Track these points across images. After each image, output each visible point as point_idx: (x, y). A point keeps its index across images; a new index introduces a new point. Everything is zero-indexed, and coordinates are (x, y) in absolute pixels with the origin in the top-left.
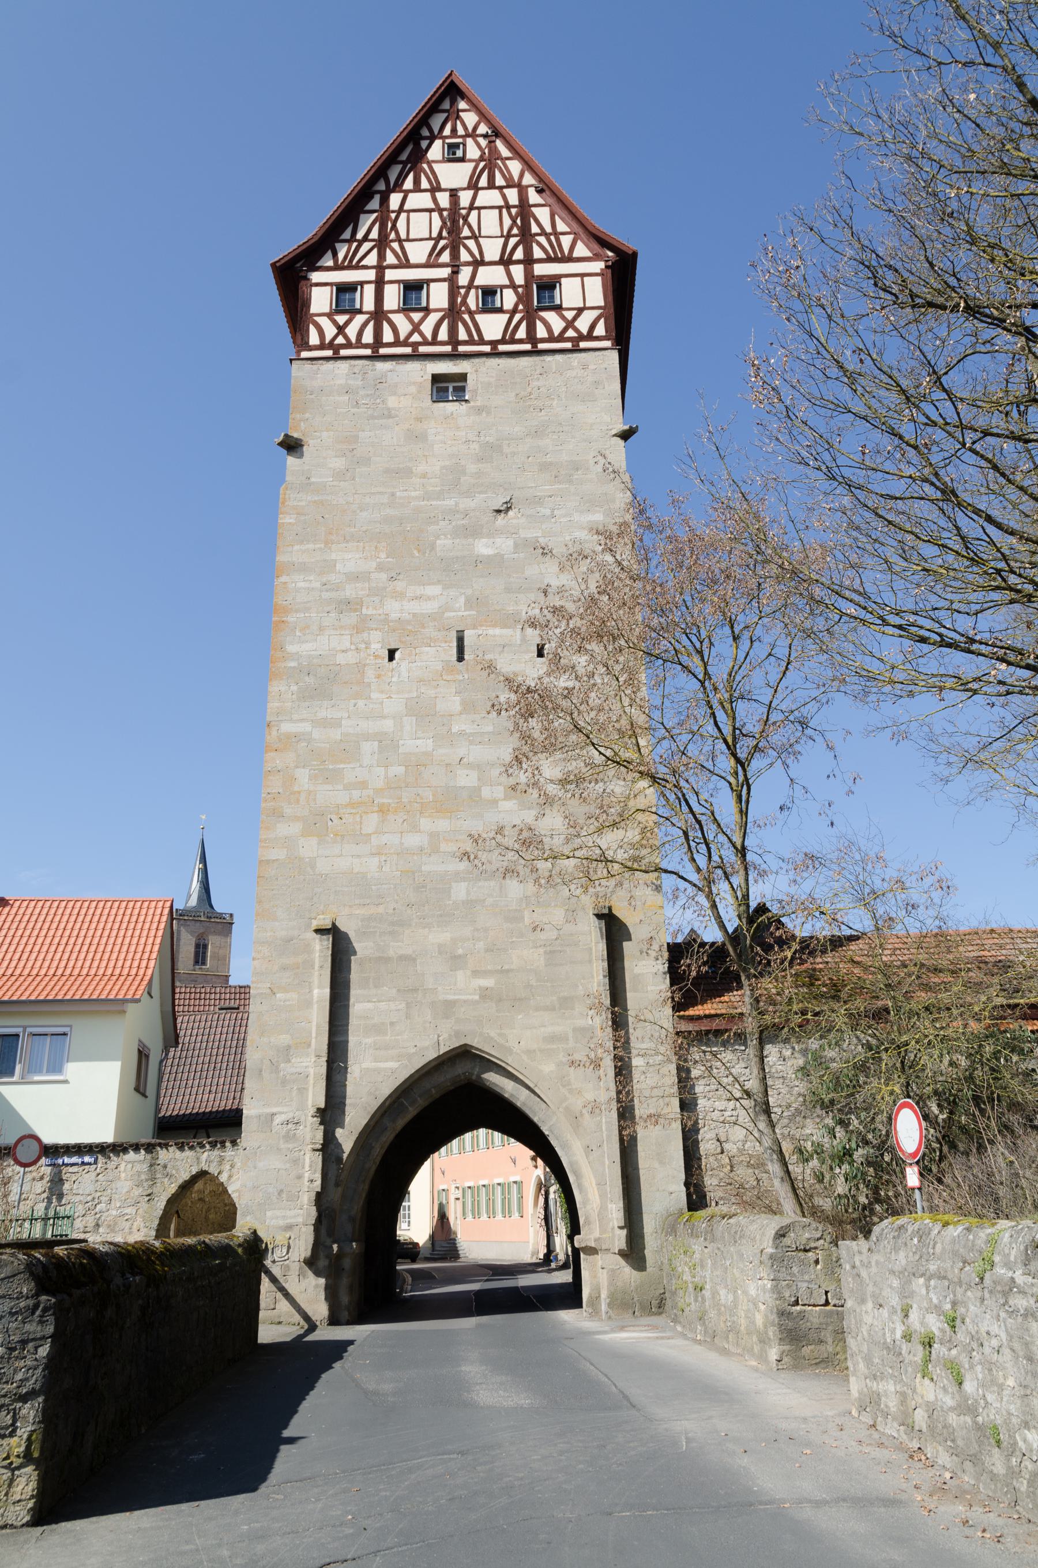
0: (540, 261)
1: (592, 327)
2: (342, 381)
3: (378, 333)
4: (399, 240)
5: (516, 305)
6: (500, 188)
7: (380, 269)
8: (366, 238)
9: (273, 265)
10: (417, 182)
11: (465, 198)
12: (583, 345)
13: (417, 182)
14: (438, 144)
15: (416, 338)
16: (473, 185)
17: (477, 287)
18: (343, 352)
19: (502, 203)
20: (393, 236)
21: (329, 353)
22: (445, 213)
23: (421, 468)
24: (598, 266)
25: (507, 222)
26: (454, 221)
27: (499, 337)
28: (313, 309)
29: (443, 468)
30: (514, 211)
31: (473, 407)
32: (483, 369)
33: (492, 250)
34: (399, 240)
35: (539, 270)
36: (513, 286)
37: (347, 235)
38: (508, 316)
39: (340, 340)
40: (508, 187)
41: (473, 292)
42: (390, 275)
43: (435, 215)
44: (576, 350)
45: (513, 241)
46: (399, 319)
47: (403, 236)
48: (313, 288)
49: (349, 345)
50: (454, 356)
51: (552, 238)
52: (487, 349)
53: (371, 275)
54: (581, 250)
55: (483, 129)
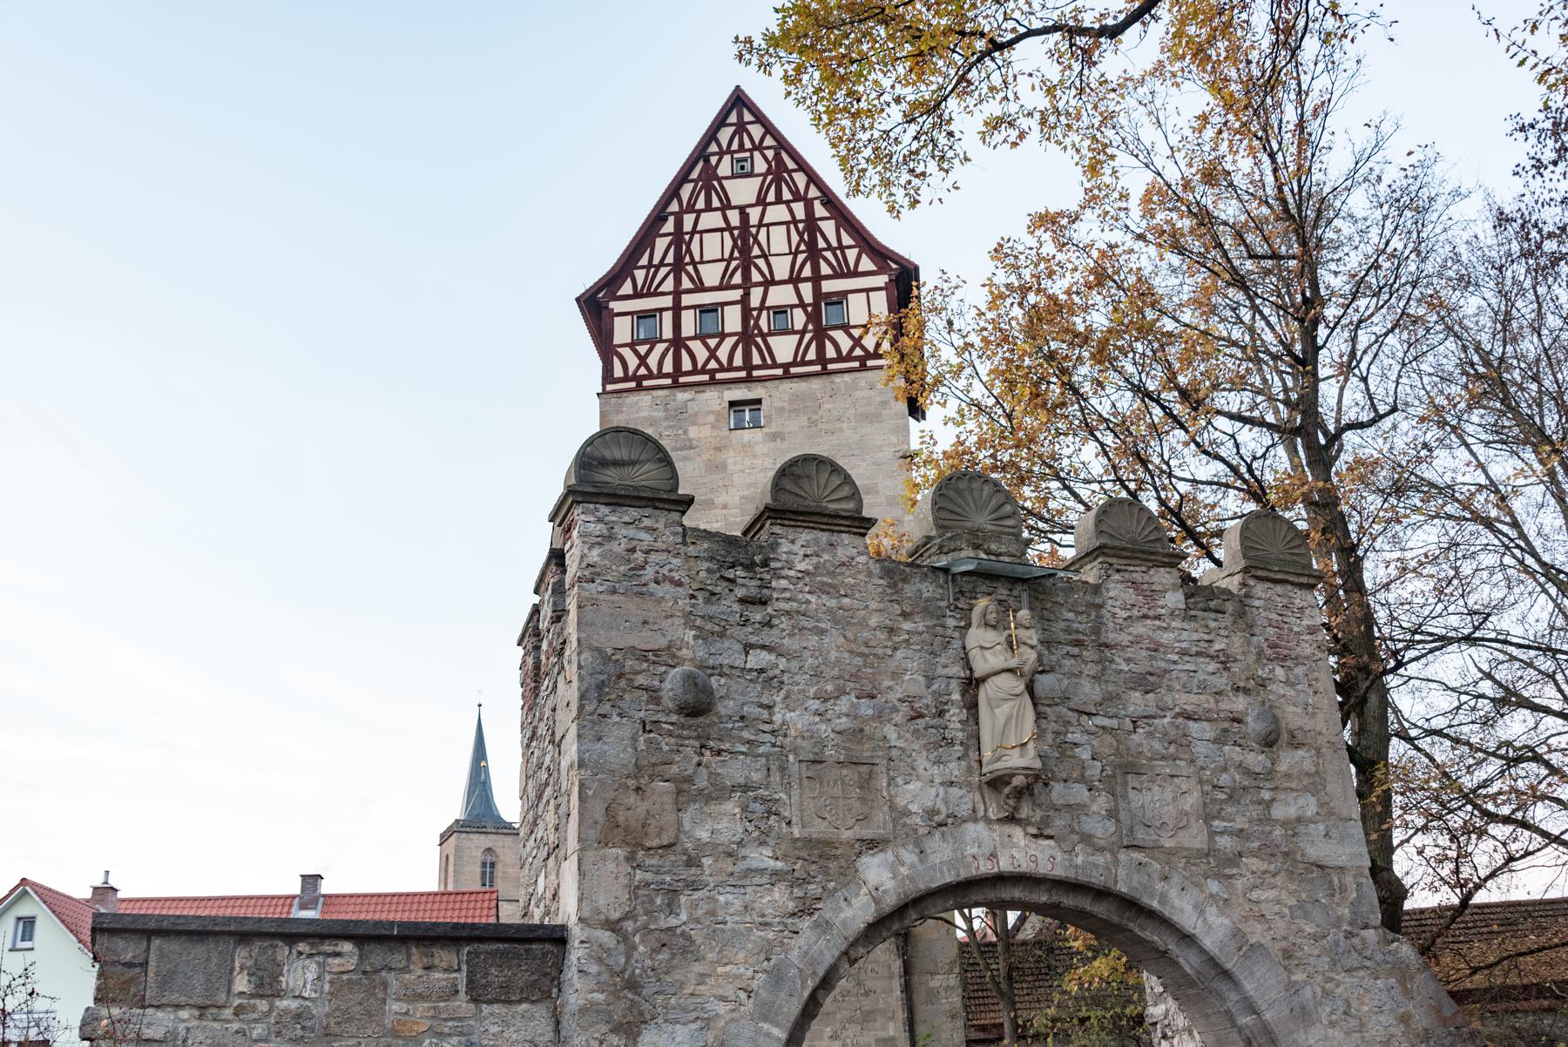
0: (828, 277)
1: (878, 345)
2: (645, 414)
4: (693, 263)
5: (806, 326)
6: (788, 203)
7: (677, 294)
8: (662, 264)
9: (578, 300)
10: (708, 201)
11: (754, 215)
12: (870, 363)
13: (708, 201)
14: (727, 158)
15: (713, 365)
16: (761, 201)
17: (769, 308)
18: (645, 383)
20: (687, 259)
22: (736, 232)
23: (722, 499)
24: (881, 280)
25: (795, 238)
26: (745, 241)
27: (790, 359)
28: (616, 342)
29: (743, 497)
30: (801, 226)
31: (767, 434)
32: (775, 393)
33: (782, 268)
34: (693, 263)
35: (828, 286)
36: (802, 305)
37: (644, 261)
38: (797, 337)
39: (643, 371)
41: (765, 313)
42: (687, 300)
43: (726, 234)
44: (863, 367)
45: (801, 257)
46: (696, 346)
47: (697, 259)
48: (616, 319)
49: (650, 376)
50: (749, 380)
52: (779, 372)
53: (667, 301)
54: (866, 264)
55: (769, 141)
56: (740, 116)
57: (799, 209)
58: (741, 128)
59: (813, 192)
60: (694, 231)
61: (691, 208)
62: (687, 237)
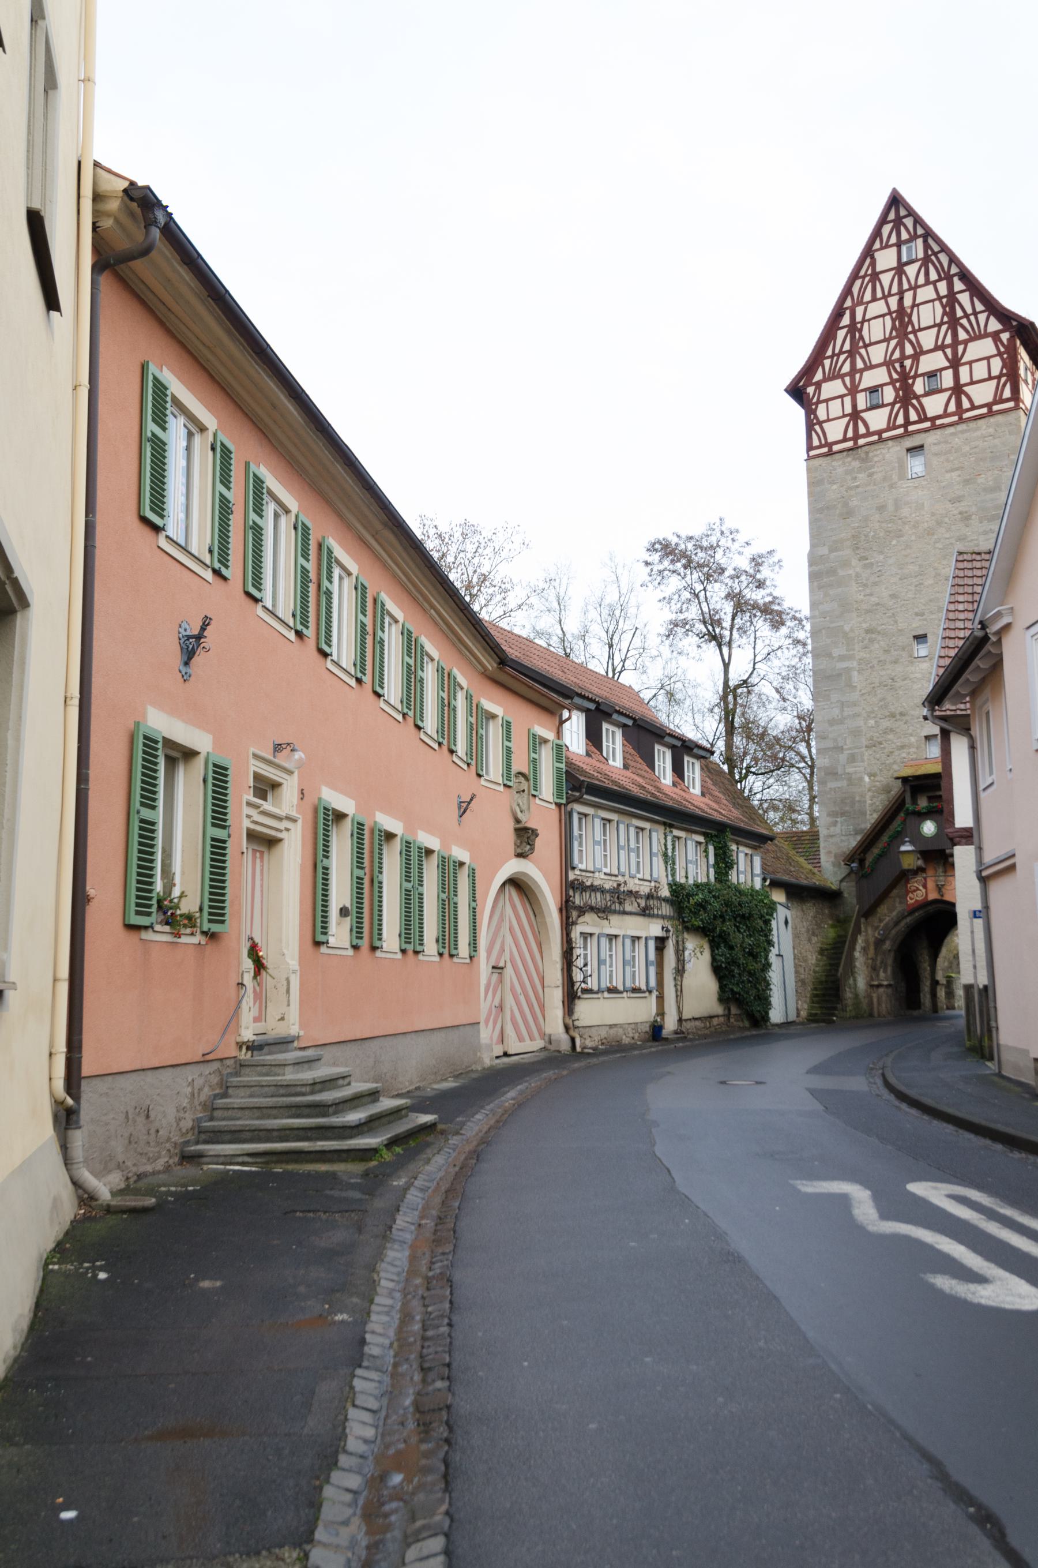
6: (934, 283)
8: (841, 352)
9: (786, 390)
21: (825, 450)
26: (902, 322)
37: (829, 353)
40: (940, 279)
51: (972, 318)
57: (943, 287)
58: (898, 222)
60: (864, 321)
61: (860, 302)
62: (859, 326)
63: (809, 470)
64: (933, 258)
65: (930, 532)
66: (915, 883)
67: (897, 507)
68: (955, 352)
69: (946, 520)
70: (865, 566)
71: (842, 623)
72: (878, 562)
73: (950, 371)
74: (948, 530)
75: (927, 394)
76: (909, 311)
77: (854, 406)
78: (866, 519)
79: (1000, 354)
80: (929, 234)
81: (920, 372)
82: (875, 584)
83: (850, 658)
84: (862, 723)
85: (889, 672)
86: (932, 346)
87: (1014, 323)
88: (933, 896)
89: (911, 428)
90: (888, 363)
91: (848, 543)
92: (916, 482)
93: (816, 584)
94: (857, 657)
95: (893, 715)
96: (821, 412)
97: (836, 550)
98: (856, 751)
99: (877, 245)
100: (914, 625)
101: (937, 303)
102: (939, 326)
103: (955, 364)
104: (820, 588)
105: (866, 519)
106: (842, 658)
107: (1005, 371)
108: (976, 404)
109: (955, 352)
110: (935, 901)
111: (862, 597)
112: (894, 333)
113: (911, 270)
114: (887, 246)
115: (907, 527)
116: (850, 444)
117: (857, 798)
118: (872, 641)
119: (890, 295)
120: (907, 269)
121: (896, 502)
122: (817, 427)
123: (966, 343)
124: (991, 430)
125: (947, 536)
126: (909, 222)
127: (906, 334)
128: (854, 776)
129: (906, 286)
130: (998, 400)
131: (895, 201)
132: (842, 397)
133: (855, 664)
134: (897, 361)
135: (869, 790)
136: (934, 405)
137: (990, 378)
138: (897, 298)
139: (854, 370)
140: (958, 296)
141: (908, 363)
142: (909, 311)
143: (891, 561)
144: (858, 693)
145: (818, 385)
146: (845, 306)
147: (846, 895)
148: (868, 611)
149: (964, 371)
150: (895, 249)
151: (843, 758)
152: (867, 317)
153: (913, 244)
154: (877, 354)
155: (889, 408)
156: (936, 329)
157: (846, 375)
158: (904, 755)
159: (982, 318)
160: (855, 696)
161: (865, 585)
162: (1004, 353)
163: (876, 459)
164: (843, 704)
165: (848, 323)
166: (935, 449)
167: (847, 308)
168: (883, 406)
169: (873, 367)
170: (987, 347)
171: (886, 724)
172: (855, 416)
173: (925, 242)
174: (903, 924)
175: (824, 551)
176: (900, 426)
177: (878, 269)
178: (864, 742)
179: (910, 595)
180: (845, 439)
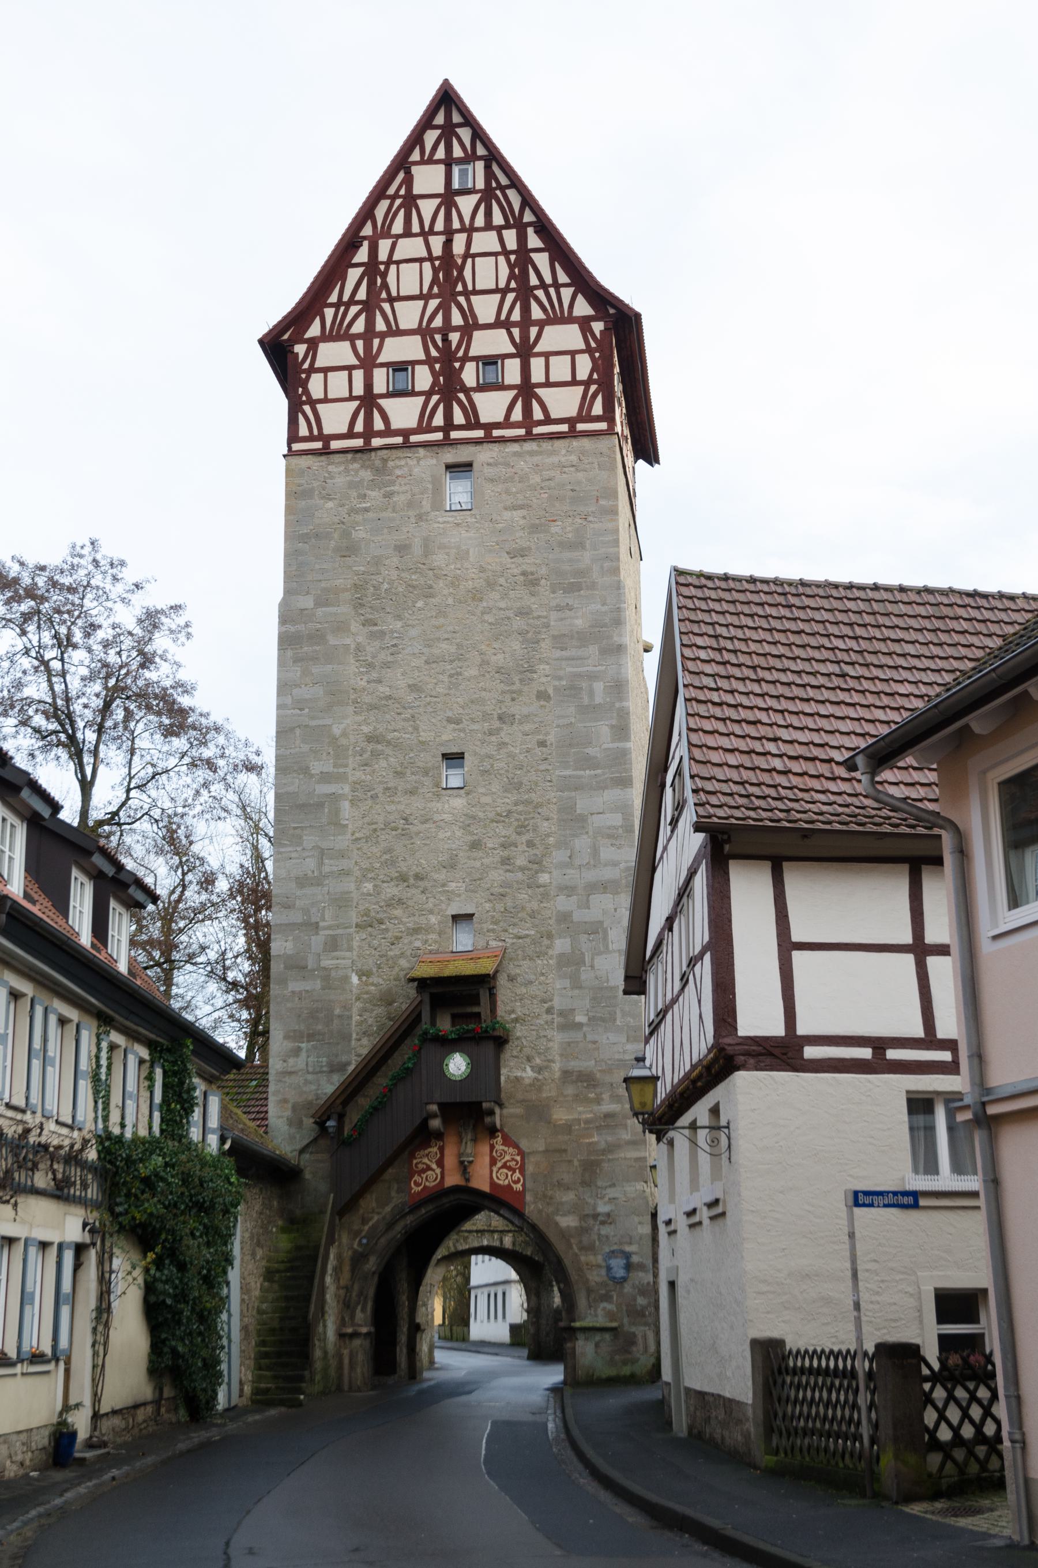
3: (369, 421)
6: (499, 229)
8: (352, 301)
9: (261, 342)
19: (499, 249)
21: (318, 445)
26: (448, 275)
37: (333, 298)
40: (507, 226)
51: (552, 290)
56: (448, 116)
57: (511, 238)
58: (448, 132)
59: (528, 217)
60: (390, 262)
61: (386, 233)
62: (382, 267)
63: (289, 472)
64: (498, 192)
65: (476, 596)
66: (427, 1158)
67: (427, 553)
68: (525, 335)
69: (502, 581)
70: (372, 635)
71: (328, 721)
72: (392, 632)
73: (517, 362)
74: (504, 596)
75: (481, 388)
76: (459, 261)
77: (368, 385)
78: (377, 561)
79: (589, 350)
80: (494, 158)
81: (472, 353)
82: (386, 665)
83: (341, 778)
84: (352, 887)
85: (402, 807)
86: (491, 320)
87: (612, 311)
88: (453, 1179)
89: (454, 435)
90: (424, 332)
91: (347, 595)
92: (459, 517)
93: (289, 653)
94: (351, 779)
95: (403, 878)
96: (315, 386)
97: (326, 603)
98: (340, 931)
99: (416, 156)
100: (444, 738)
101: (501, 259)
102: (504, 292)
103: (525, 351)
104: (296, 660)
105: (377, 561)
106: (326, 778)
107: (595, 376)
108: (553, 416)
109: (525, 335)
110: (456, 1189)
111: (363, 683)
112: (436, 290)
113: (466, 204)
114: (431, 161)
115: (441, 583)
116: (359, 442)
117: (337, 1011)
118: (376, 755)
119: (432, 232)
120: (460, 200)
121: (426, 542)
122: (307, 408)
123: (541, 324)
124: (573, 458)
125: (502, 605)
126: (465, 134)
127: (454, 295)
128: (333, 974)
129: (456, 225)
130: (585, 415)
131: (447, 98)
132: (350, 368)
133: (347, 789)
134: (437, 330)
135: (358, 999)
136: (492, 406)
137: (574, 382)
138: (442, 238)
139: (370, 332)
140: (533, 255)
141: (454, 337)
142: (459, 261)
143: (413, 632)
144: (349, 836)
145: (313, 345)
146: (363, 234)
147: (307, 1175)
148: (372, 707)
149: (537, 366)
150: (442, 168)
151: (317, 941)
152: (395, 258)
153: (470, 167)
154: (409, 315)
155: (423, 398)
156: (498, 296)
157: (358, 336)
158: (418, 944)
159: (567, 293)
160: (342, 841)
161: (371, 666)
162: (596, 350)
163: (398, 472)
164: (322, 854)
165: (366, 260)
166: (489, 471)
167: (365, 238)
168: (413, 393)
169: (400, 333)
170: (569, 336)
171: (391, 890)
172: (369, 401)
173: (488, 168)
174: (399, 1227)
175: (307, 602)
176: (437, 429)
177: (416, 191)
178: (354, 917)
179: (441, 689)
180: (350, 434)
